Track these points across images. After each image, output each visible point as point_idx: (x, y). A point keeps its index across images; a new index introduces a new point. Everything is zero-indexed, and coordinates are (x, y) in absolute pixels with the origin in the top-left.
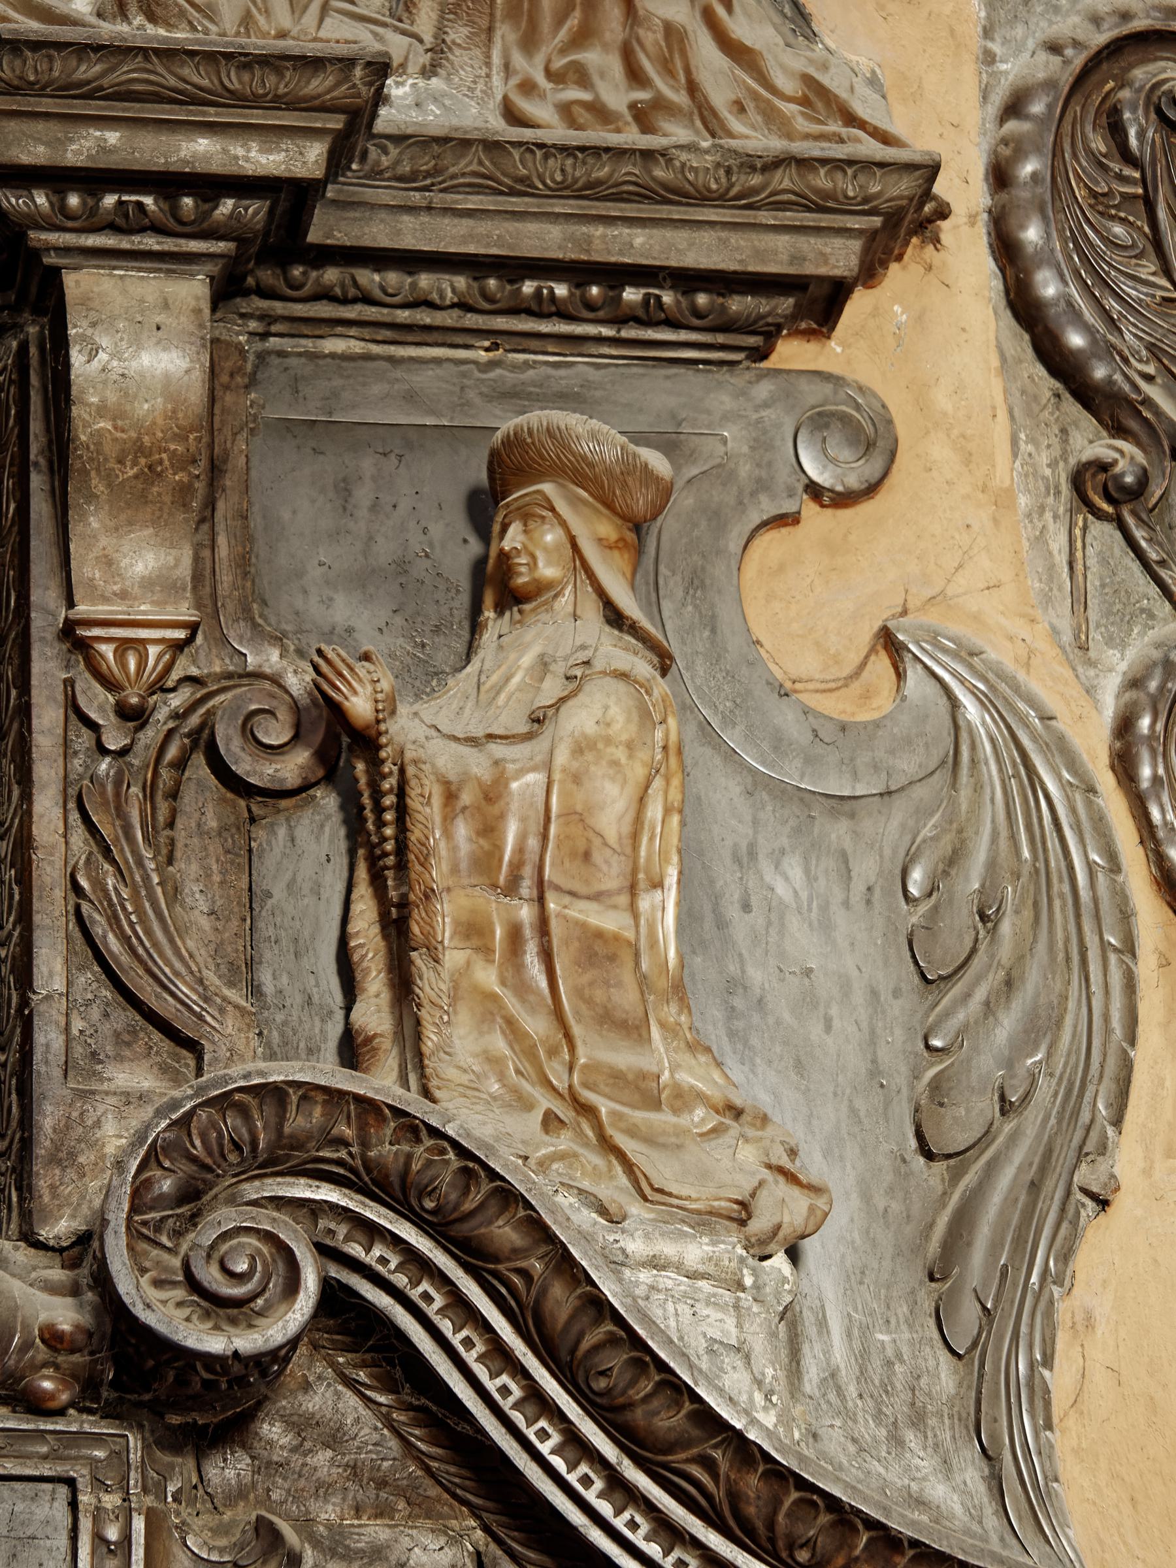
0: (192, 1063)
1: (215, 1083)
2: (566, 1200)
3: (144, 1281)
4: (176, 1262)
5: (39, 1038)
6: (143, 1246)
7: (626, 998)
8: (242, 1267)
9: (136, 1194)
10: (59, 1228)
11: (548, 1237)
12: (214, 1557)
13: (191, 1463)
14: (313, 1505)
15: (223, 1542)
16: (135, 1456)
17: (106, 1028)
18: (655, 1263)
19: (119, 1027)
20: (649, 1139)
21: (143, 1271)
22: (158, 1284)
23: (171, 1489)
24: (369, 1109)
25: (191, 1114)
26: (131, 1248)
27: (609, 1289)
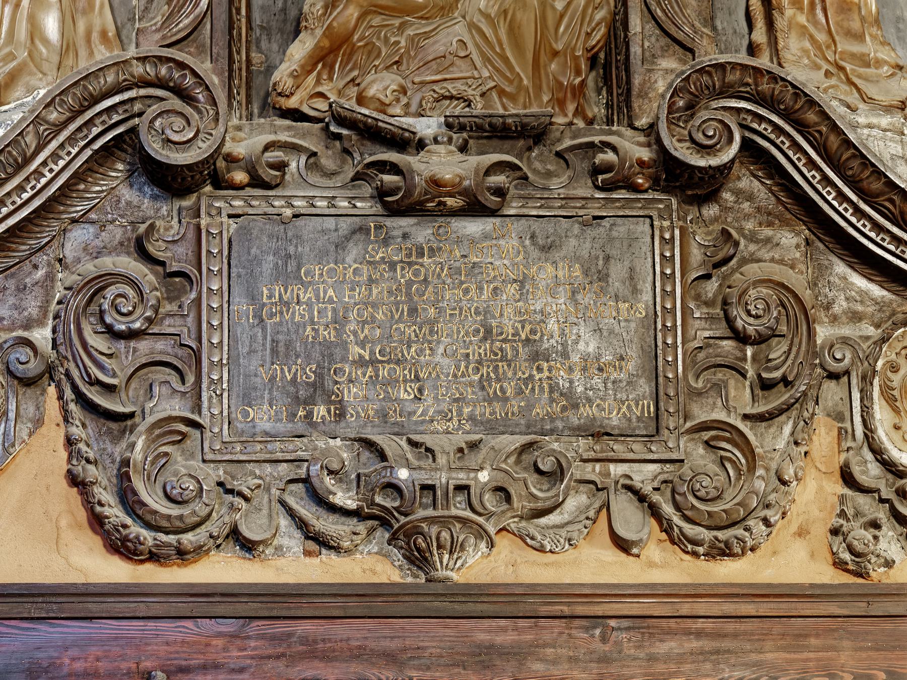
0: (691, 57)
1: (698, 64)
2: (835, 103)
3: (674, 140)
4: (686, 132)
5: (632, 50)
6: (673, 127)
7: (856, 25)
8: (711, 133)
9: (669, 107)
10: (643, 122)
11: (828, 118)
12: (706, 244)
13: (696, 209)
14: (743, 223)
15: (709, 238)
16: (675, 207)
17: (658, 45)
18: (870, 126)
19: (663, 44)
20: (866, 79)
21: (673, 136)
22: (679, 141)
23: (689, 218)
24: (757, 71)
25: (689, 75)
26: (668, 128)
27: (852, 137)
